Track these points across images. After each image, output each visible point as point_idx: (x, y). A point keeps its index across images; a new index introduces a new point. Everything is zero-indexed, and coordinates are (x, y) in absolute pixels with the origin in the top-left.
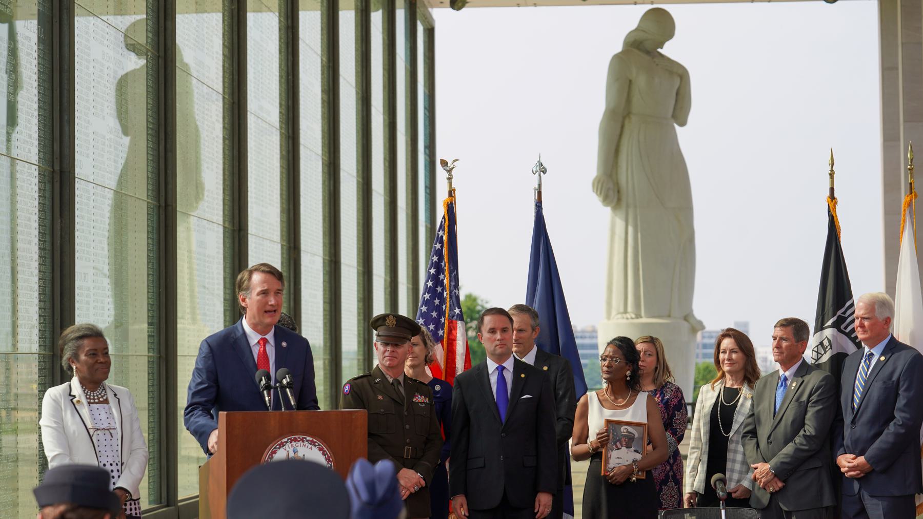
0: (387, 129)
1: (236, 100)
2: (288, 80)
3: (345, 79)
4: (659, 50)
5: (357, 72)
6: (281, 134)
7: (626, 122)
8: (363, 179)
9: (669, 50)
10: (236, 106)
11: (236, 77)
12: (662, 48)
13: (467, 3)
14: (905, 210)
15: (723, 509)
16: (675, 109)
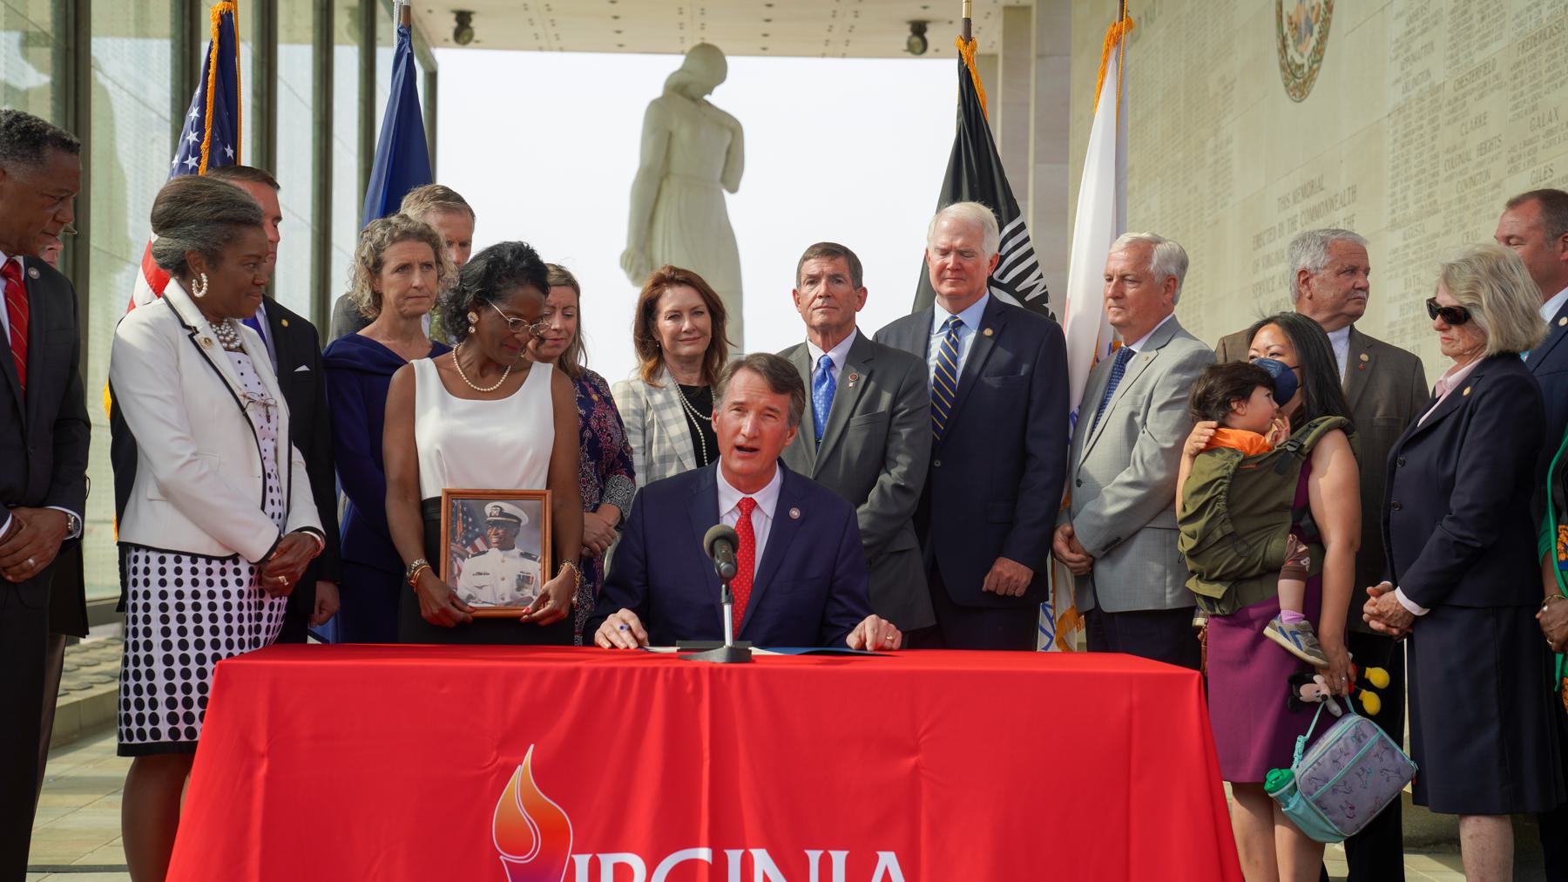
0: (362, 176)
1: (72, 45)
2: (183, 54)
3: (290, 88)
4: (707, 97)
5: (314, 88)
6: (173, 126)
7: (665, 183)
8: (320, 227)
9: (719, 98)
10: (72, 56)
11: (71, 11)
12: (710, 94)
13: (477, 42)
14: (1107, 52)
15: (728, 601)
16: (724, 172)
